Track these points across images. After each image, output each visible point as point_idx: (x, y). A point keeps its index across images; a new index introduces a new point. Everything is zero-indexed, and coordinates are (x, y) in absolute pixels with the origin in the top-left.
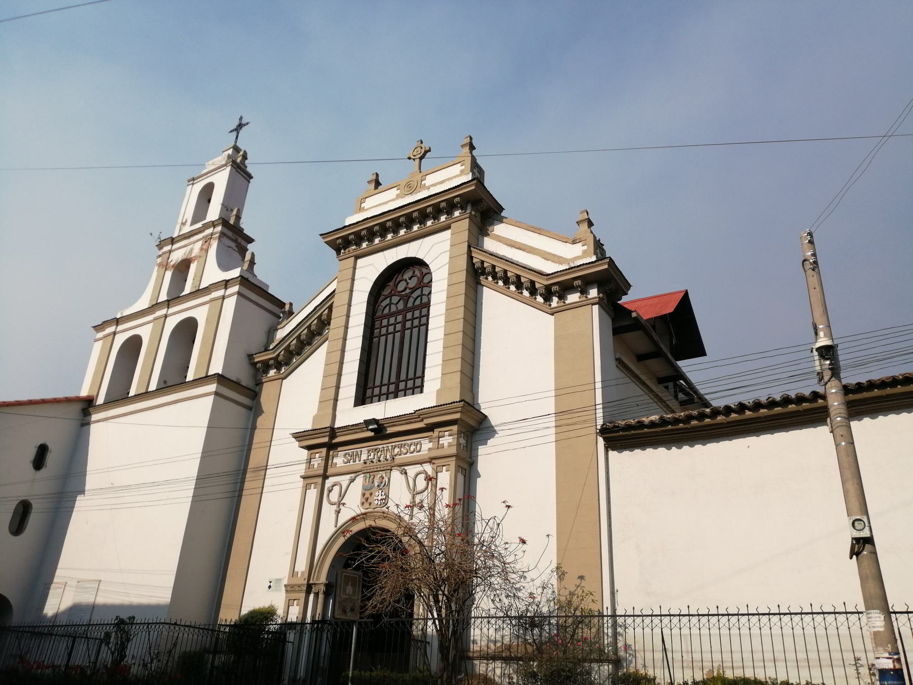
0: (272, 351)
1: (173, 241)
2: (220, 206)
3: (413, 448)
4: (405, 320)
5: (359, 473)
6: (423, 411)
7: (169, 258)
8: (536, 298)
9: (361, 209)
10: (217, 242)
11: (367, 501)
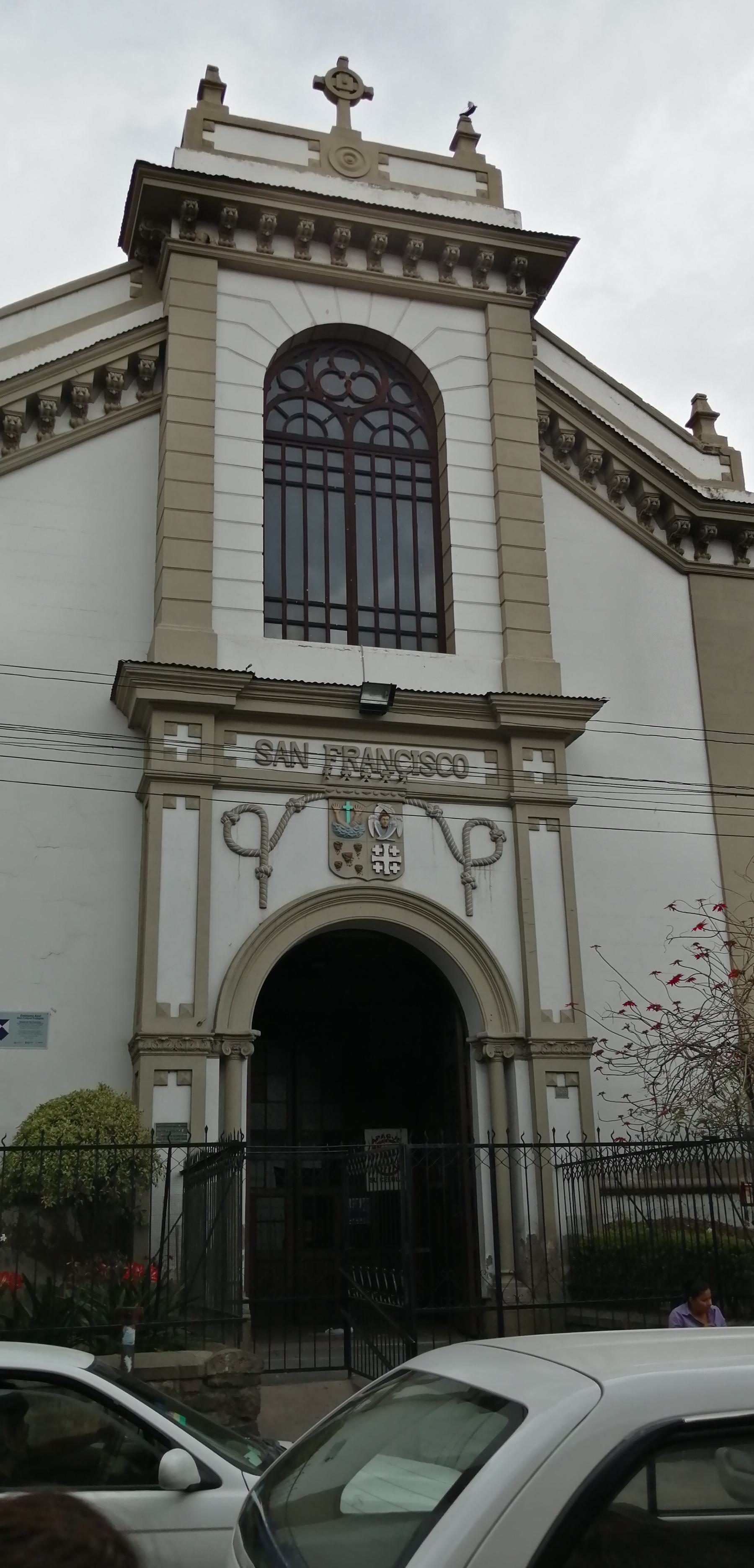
3: (445, 766)
4: (349, 472)
5: (317, 796)
8: (652, 531)
9: (208, 147)
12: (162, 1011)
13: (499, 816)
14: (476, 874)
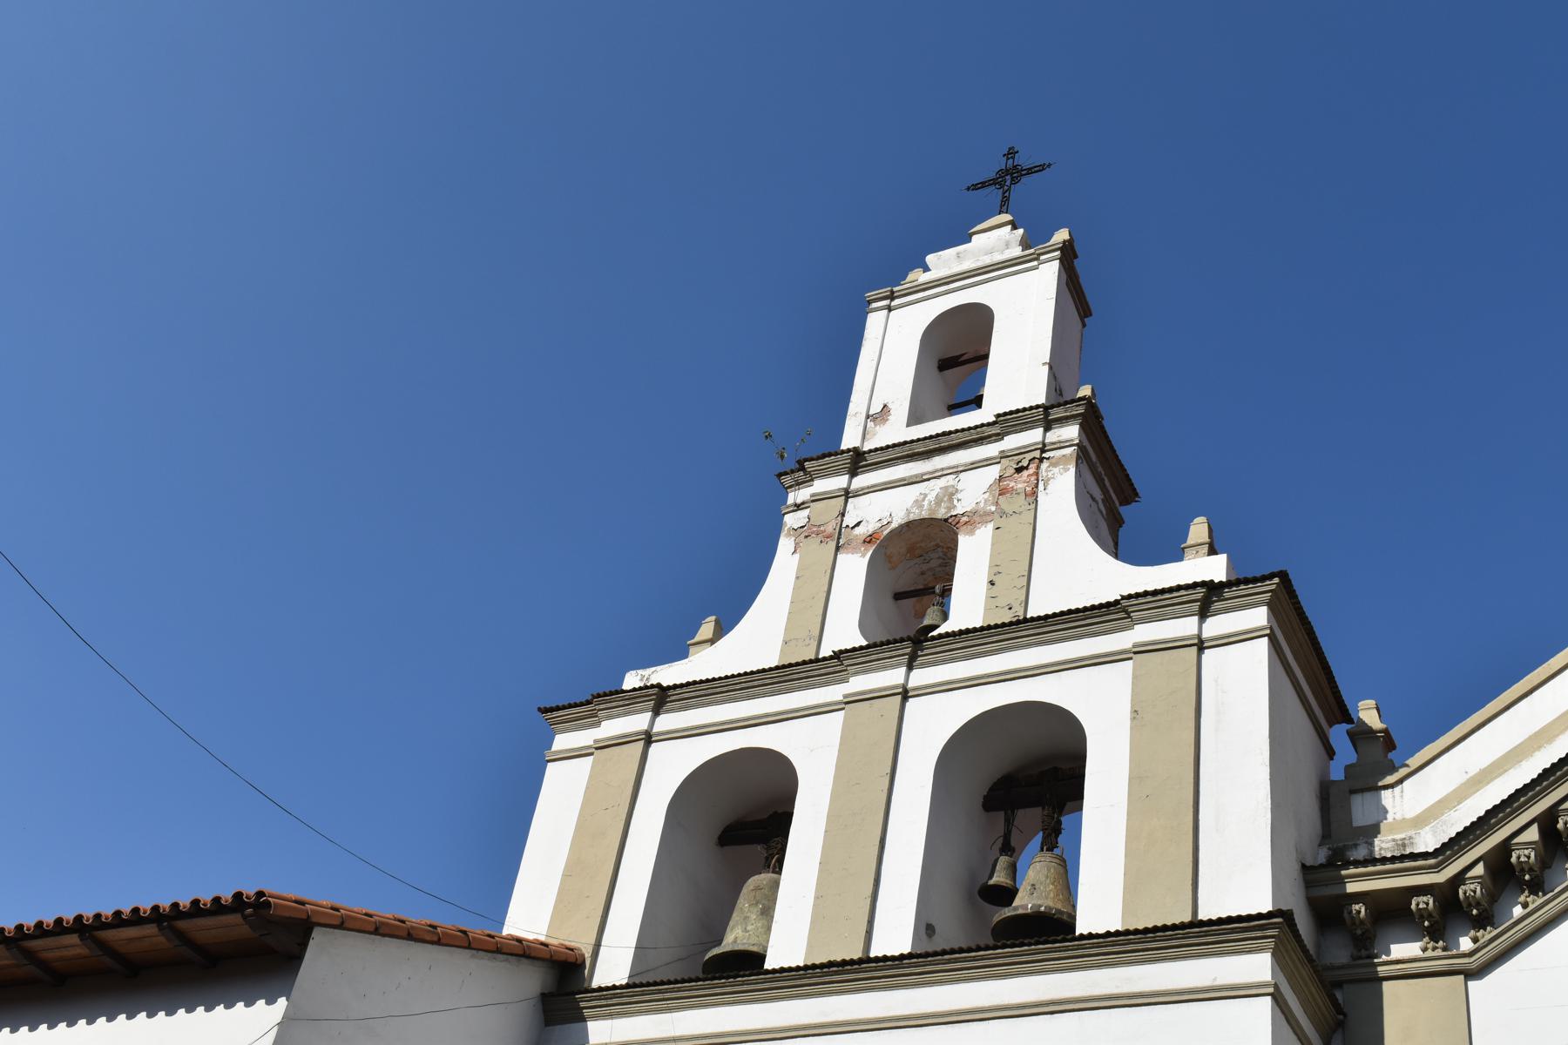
0: (1432, 861)
1: (858, 461)
2: (1047, 367)
7: (843, 515)
10: (1072, 470)
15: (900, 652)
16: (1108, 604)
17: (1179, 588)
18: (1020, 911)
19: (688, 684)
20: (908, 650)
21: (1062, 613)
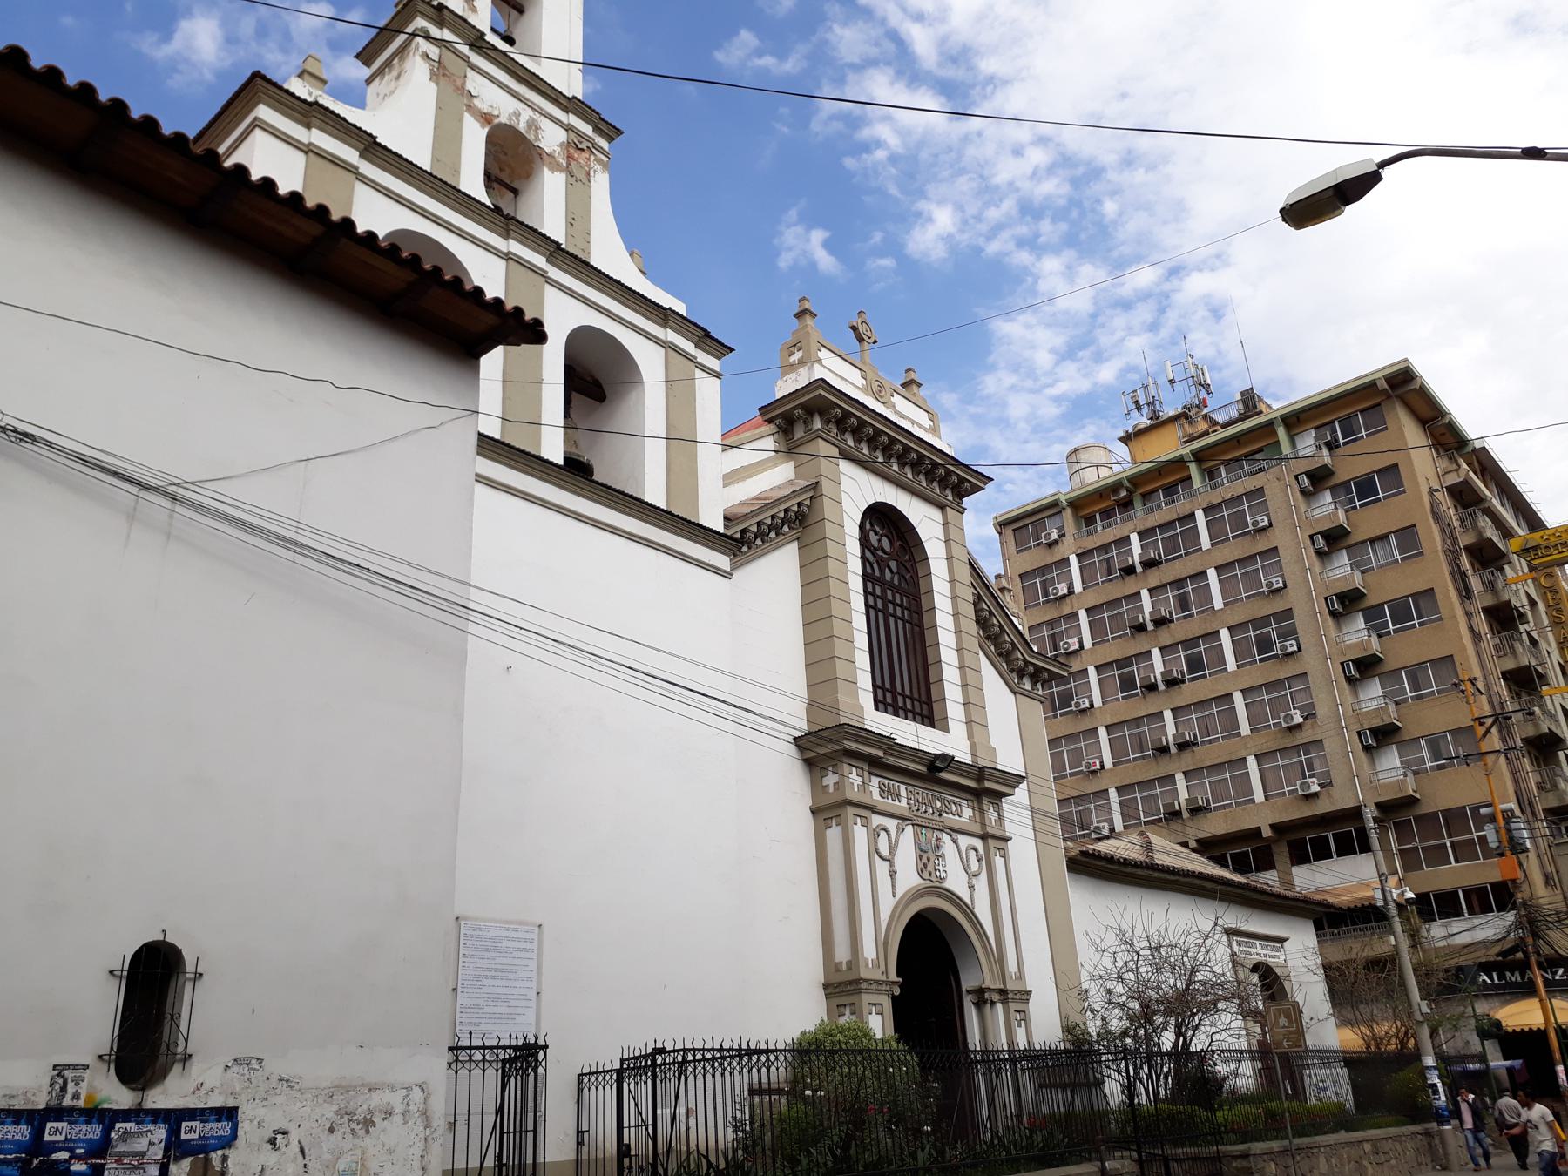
3: (954, 808)
6: (991, 771)
11: (926, 868)
12: (866, 960)
13: (978, 843)
14: (974, 881)
15: (546, 246)
16: (661, 307)
17: (695, 324)
18: (582, 459)
19: (396, 154)
20: (552, 249)
21: (638, 294)
